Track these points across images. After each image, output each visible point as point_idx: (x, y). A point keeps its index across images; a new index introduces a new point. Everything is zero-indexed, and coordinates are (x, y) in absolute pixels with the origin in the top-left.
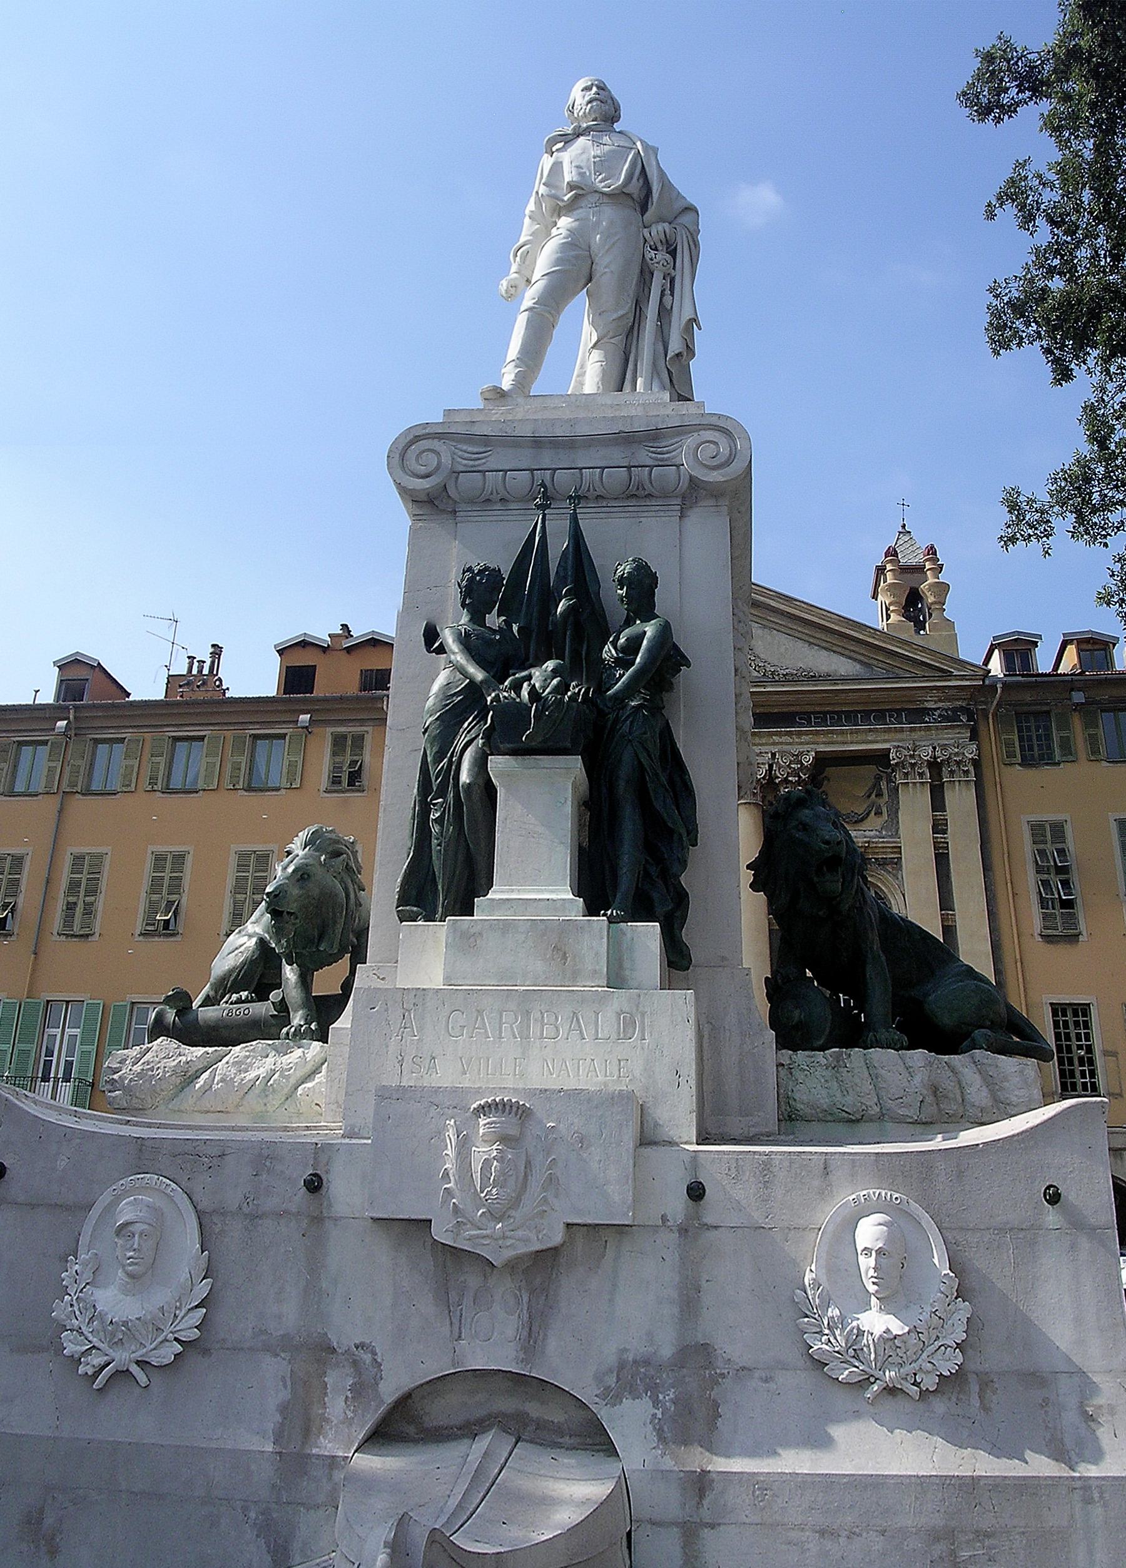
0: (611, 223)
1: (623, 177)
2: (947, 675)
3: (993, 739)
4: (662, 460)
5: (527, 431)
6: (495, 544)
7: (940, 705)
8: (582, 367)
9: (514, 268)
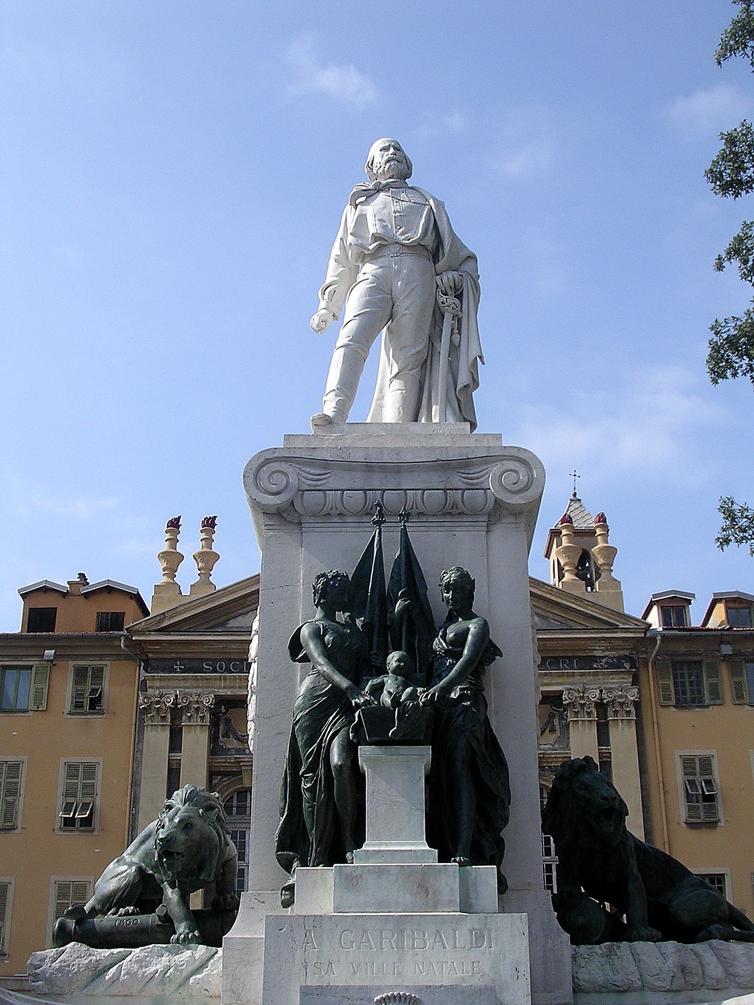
0: (411, 271)
1: (420, 232)
2: (614, 628)
3: (652, 684)
4: (472, 484)
5: (360, 457)
6: (338, 552)
7: (607, 653)
8: (381, 392)
9: (323, 304)
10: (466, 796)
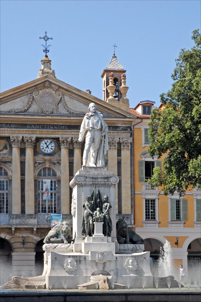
7: (122, 125)
10: (107, 227)
